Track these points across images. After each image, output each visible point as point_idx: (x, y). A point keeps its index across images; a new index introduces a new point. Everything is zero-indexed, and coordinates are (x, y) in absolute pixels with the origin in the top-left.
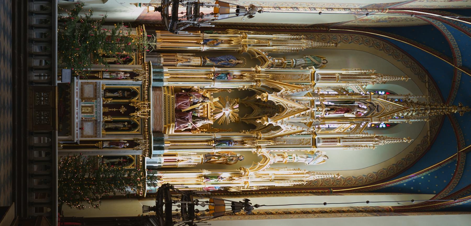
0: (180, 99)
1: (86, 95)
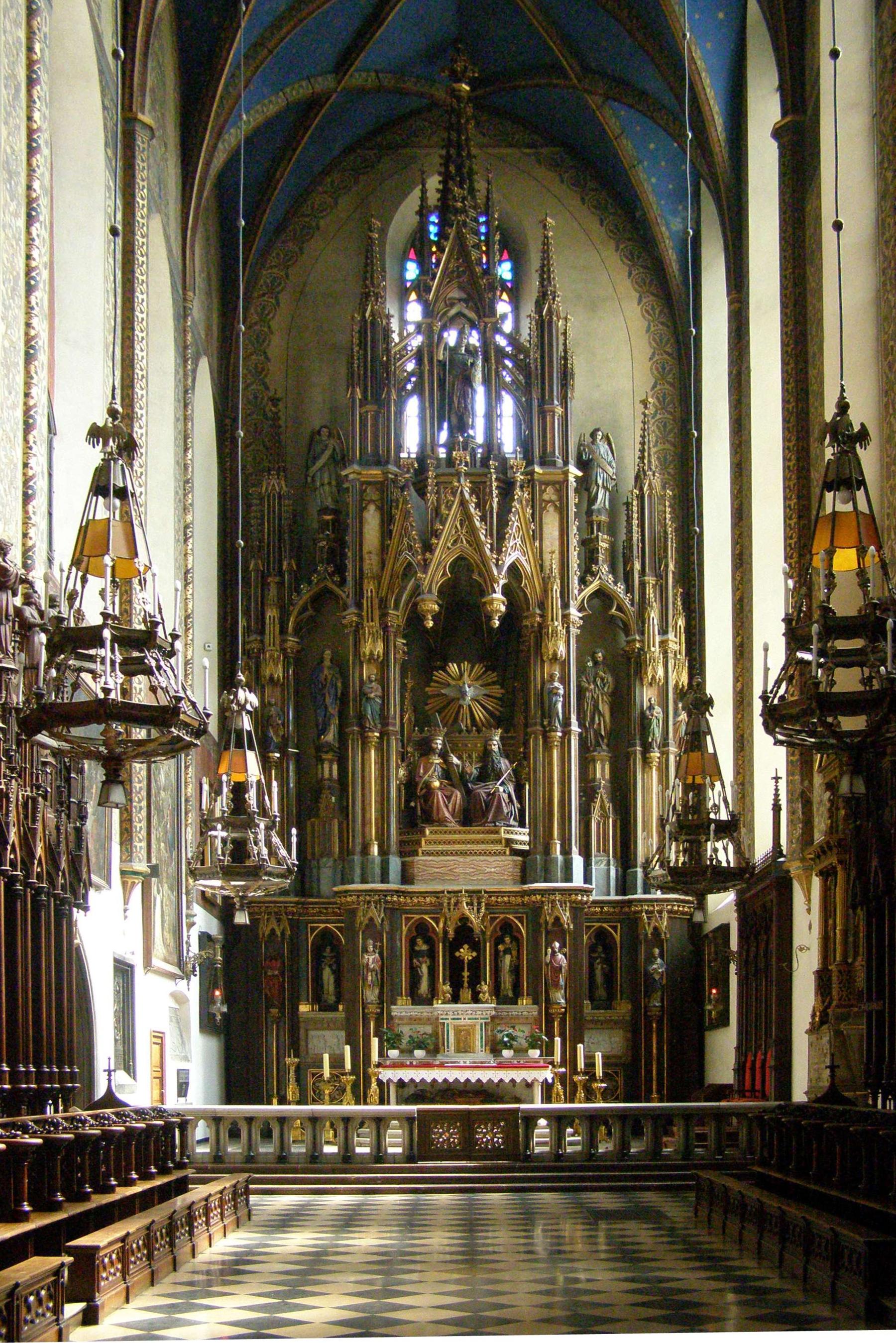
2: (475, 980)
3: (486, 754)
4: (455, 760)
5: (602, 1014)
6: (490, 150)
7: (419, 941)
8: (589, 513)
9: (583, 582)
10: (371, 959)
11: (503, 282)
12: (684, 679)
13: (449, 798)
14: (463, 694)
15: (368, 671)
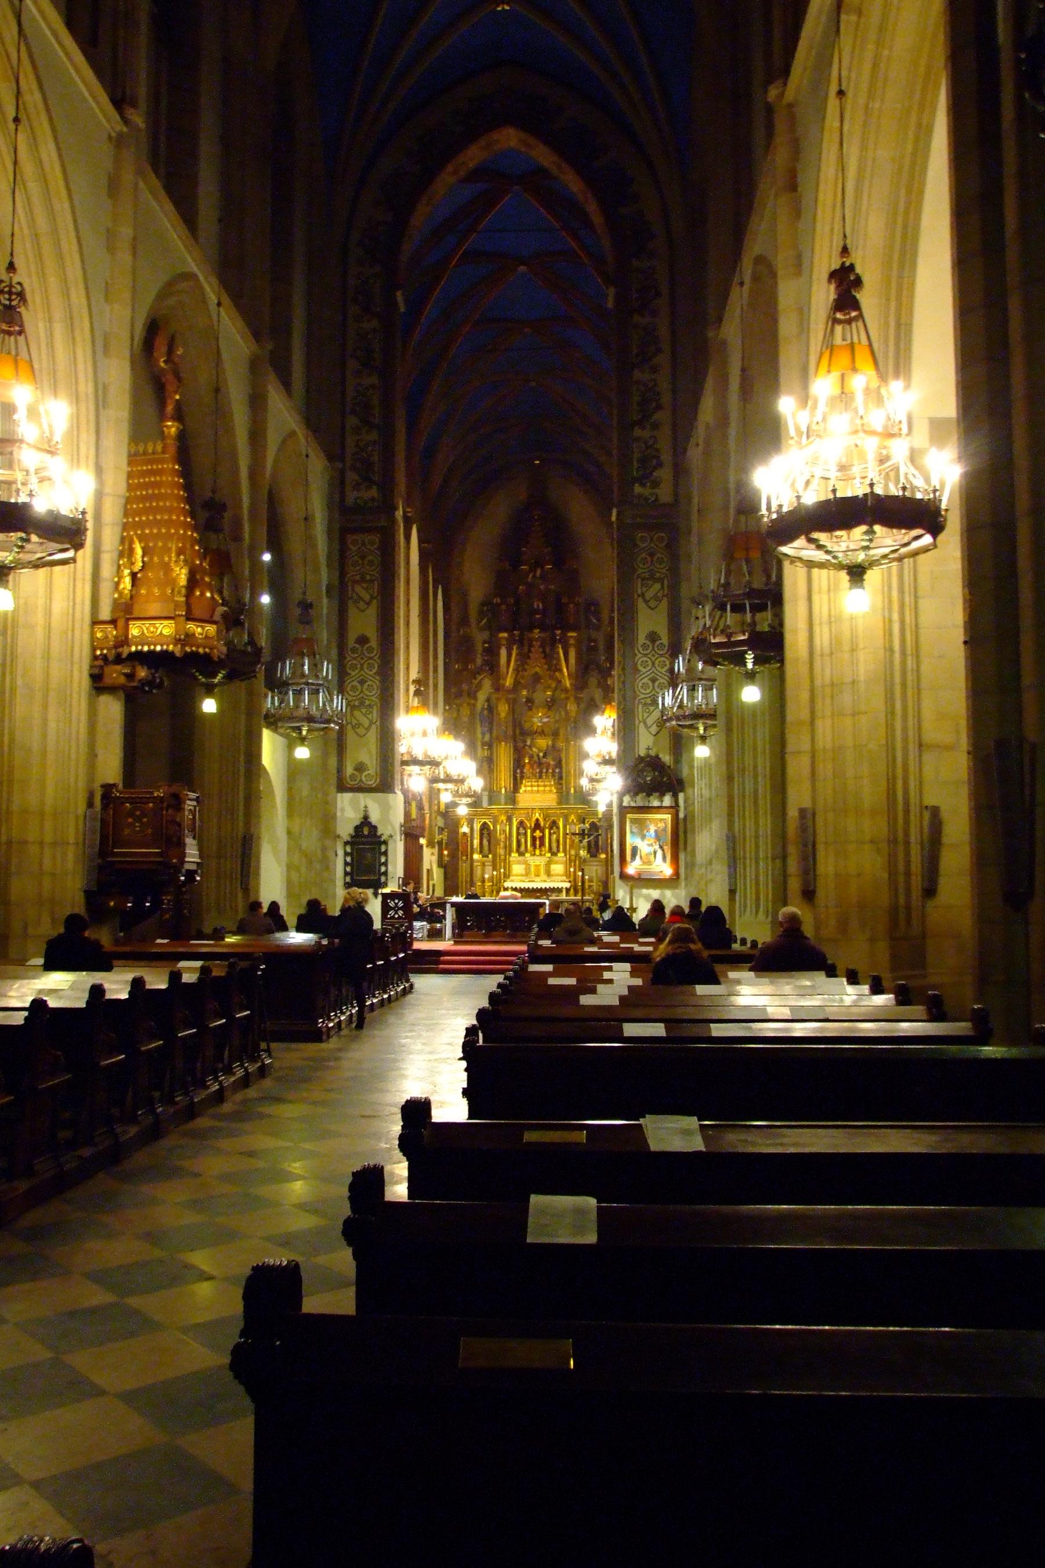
1: (523, 872)
2: (542, 844)
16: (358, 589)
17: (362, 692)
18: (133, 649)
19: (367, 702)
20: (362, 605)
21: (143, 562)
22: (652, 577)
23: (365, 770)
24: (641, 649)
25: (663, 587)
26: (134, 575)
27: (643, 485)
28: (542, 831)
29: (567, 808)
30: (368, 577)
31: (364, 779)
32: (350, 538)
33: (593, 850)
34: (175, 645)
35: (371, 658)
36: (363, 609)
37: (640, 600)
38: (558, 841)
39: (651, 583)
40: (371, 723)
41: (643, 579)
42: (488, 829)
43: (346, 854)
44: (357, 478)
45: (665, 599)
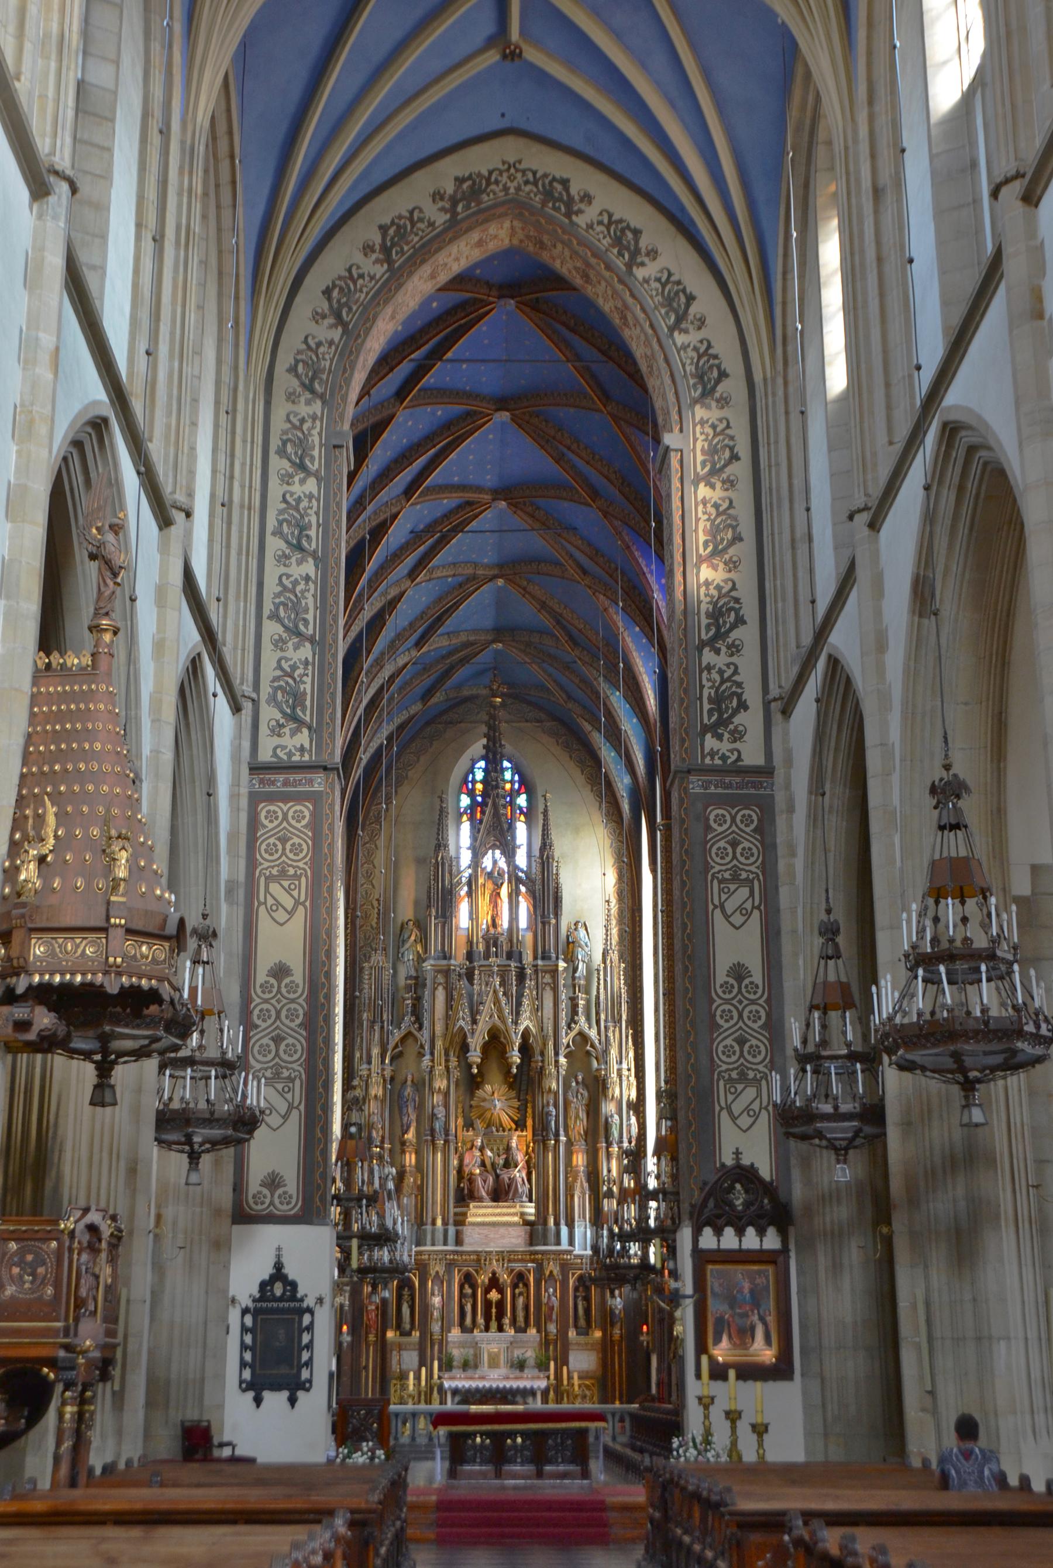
0: (476, 1194)
3: (508, 1149)
4: (489, 1153)
5: (582, 1339)
6: (515, 724)
7: (466, 1286)
8: (574, 978)
9: (569, 1027)
10: (437, 1300)
11: (521, 808)
12: (633, 1095)
13: (485, 1181)
14: (495, 1106)
15: (437, 1099)
16: (274, 888)
17: (277, 1055)
18: (37, 979)
19: (286, 1073)
20: (281, 915)
21: (56, 837)
22: (735, 878)
23: (278, 1186)
24: (719, 991)
25: (752, 893)
26: (42, 860)
27: (720, 737)
28: (501, 1291)
29: (543, 1253)
30: (291, 871)
31: (277, 1201)
32: (264, 809)
33: (582, 1322)
34: (106, 973)
35: (293, 1001)
36: (282, 921)
37: (718, 912)
38: (526, 1307)
39: (732, 887)
40: (291, 1107)
41: (720, 882)
42: (412, 1287)
43: (244, 1329)
44: (278, 716)
45: (756, 913)
